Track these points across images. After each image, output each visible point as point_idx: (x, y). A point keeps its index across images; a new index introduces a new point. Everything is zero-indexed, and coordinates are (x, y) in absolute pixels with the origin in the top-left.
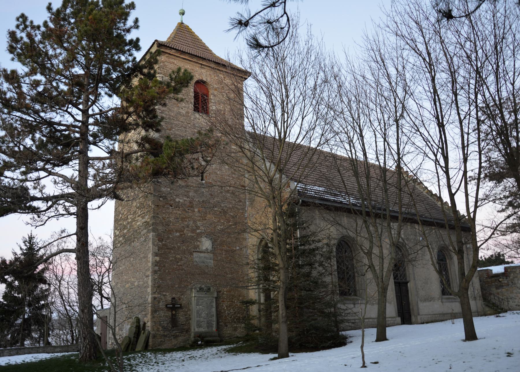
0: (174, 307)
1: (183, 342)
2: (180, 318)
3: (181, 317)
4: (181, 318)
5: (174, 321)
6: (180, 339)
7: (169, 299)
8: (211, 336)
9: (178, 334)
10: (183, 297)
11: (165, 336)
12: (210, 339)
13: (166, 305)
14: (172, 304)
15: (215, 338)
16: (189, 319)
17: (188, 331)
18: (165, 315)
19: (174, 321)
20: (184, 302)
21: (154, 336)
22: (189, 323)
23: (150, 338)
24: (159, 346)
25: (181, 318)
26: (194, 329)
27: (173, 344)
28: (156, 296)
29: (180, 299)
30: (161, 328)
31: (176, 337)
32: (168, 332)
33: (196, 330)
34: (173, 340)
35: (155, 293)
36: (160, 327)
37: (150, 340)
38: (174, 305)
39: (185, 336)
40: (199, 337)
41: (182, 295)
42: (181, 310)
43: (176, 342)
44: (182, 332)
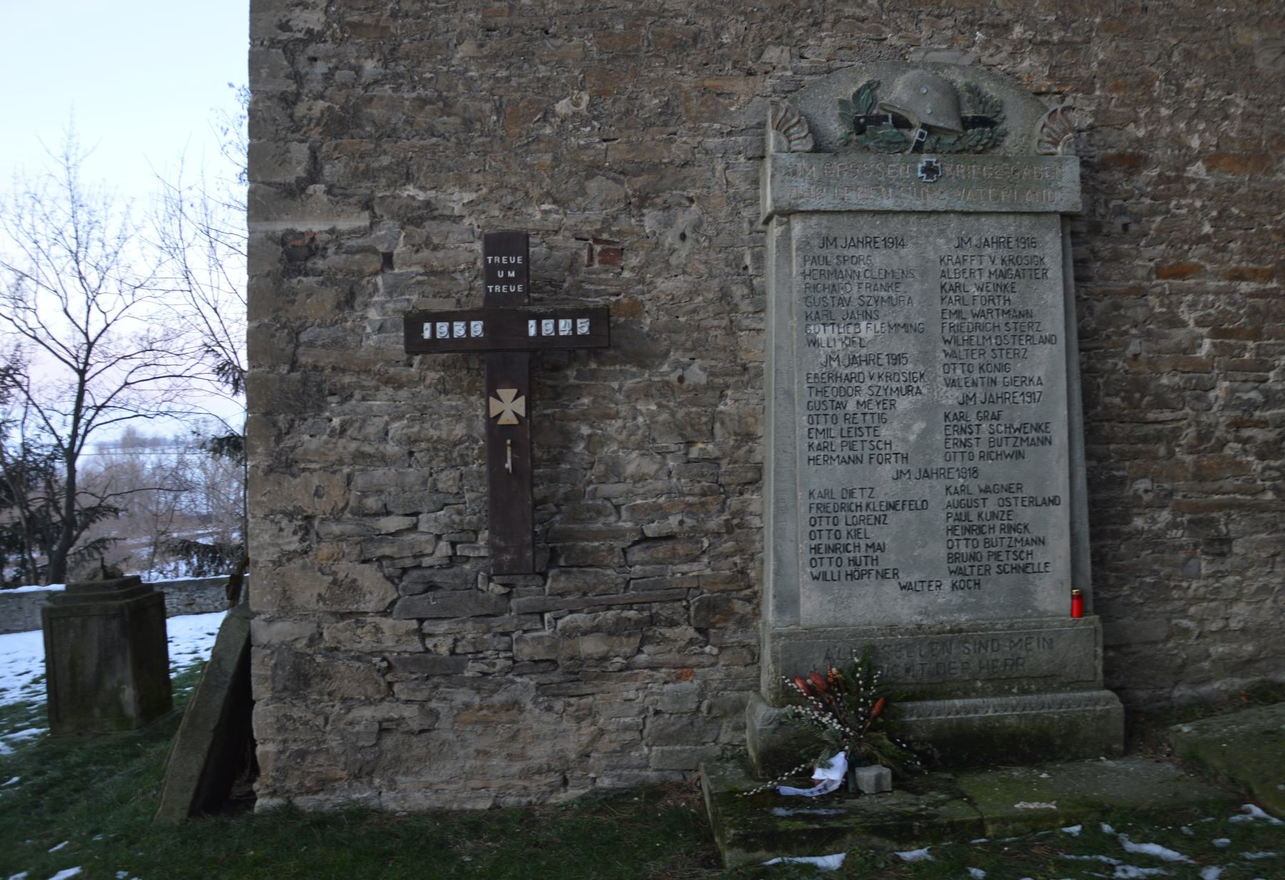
0: (536, 346)
1: (664, 738)
2: (614, 471)
3: (628, 450)
4: (634, 463)
5: (534, 514)
6: (623, 703)
7: (463, 249)
8: (1001, 682)
9: (590, 646)
10: (650, 221)
11: (438, 671)
12: (987, 708)
13: (412, 322)
14: (494, 312)
15: (1051, 705)
16: (729, 481)
17: (721, 610)
18: (416, 439)
19: (534, 514)
20: (665, 285)
21: (300, 677)
22: (737, 526)
23: (260, 691)
24: (362, 773)
25: (634, 463)
26: (787, 602)
27: (540, 753)
28: (316, 226)
29: (612, 255)
30: (374, 587)
31: (567, 677)
32: (470, 631)
33: (814, 606)
34: (535, 718)
35: (294, 192)
36: (369, 577)
37: (263, 716)
38: (502, 316)
39: (682, 671)
40: (832, 691)
41: (643, 200)
42: (624, 380)
43: (574, 740)
44: (645, 630)
